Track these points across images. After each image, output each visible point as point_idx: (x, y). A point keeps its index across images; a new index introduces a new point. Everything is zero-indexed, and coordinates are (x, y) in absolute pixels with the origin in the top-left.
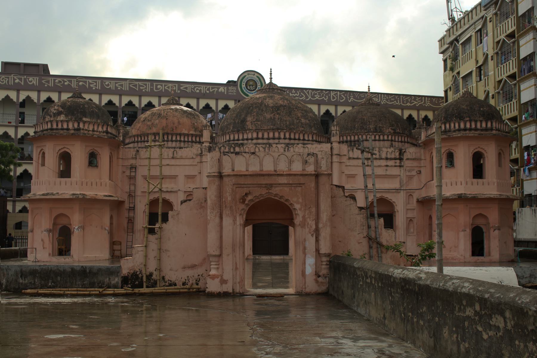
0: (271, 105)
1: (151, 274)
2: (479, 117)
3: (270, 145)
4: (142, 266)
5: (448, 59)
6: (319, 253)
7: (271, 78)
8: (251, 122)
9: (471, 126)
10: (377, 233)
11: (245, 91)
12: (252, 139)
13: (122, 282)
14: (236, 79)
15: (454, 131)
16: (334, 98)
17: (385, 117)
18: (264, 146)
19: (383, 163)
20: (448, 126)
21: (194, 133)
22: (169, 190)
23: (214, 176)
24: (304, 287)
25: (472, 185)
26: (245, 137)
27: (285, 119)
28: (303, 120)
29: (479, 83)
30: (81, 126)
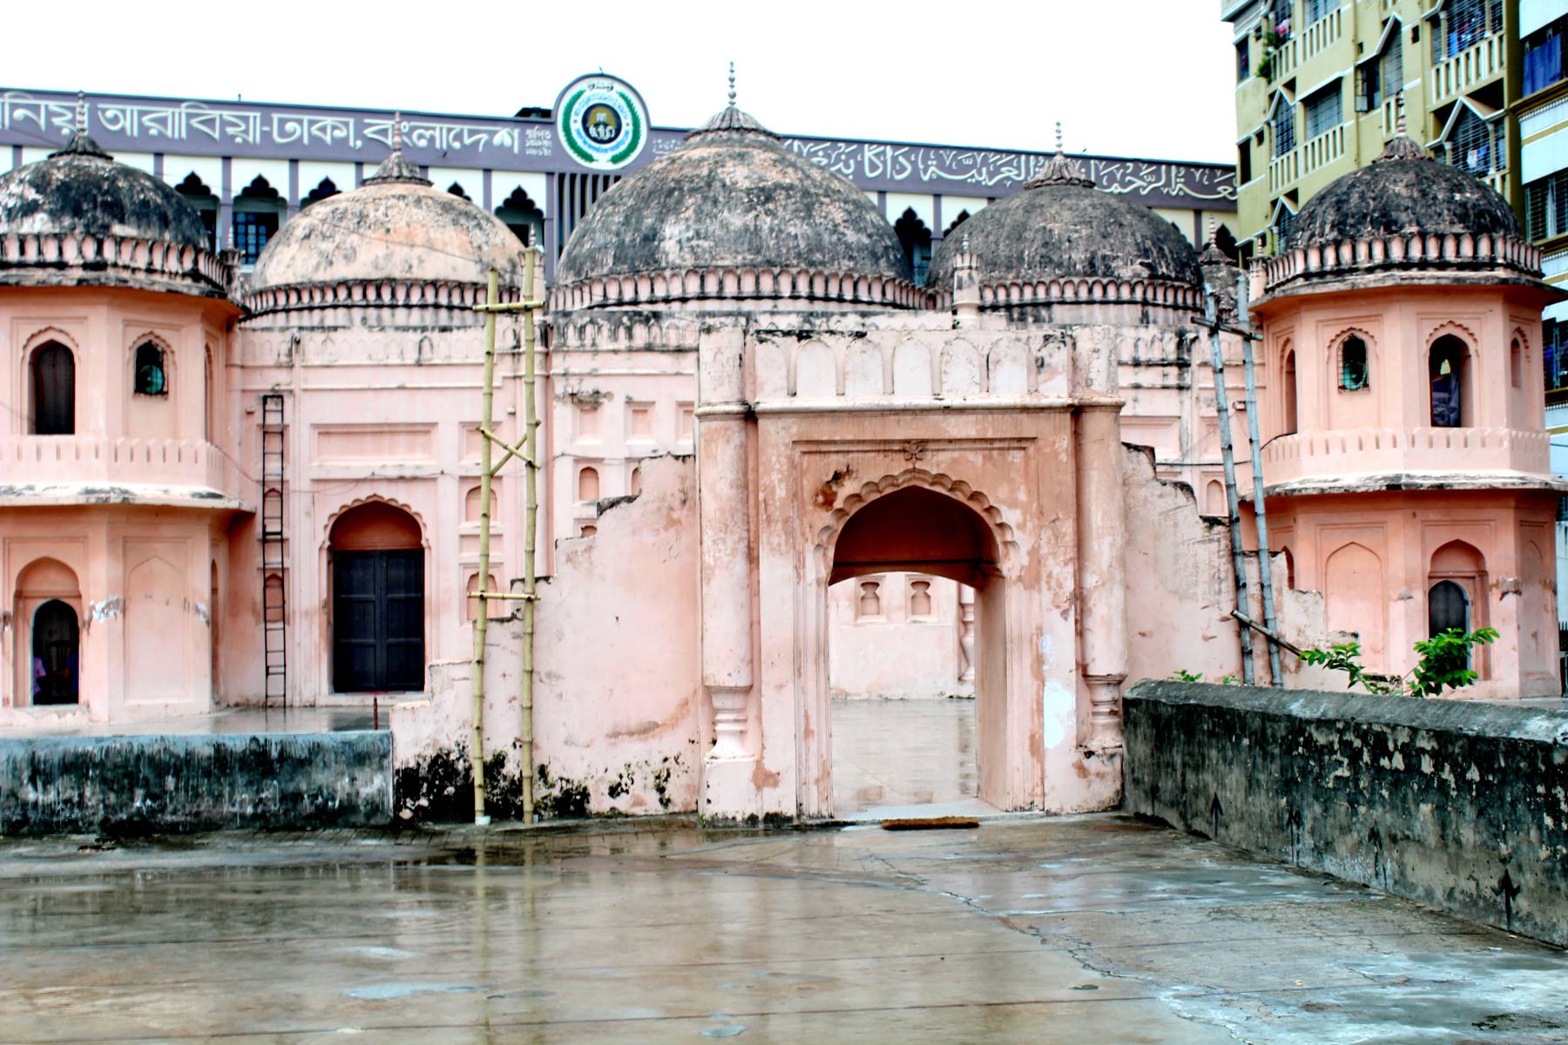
0: (746, 184)
1: (499, 761)
2: (1452, 223)
4: (470, 732)
5: (1252, 41)
6: (1086, 676)
8: (680, 241)
9: (1424, 251)
10: (1267, 603)
11: (580, 143)
12: (684, 300)
13: (397, 788)
14: (547, 105)
15: (1370, 270)
16: (873, 167)
17: (1121, 225)
20: (1346, 252)
22: (407, 473)
23: (727, 413)
24: (1038, 790)
25: (1431, 445)
26: (660, 292)
27: (793, 230)
28: (851, 236)
29: (1363, 118)
30: (109, 252)
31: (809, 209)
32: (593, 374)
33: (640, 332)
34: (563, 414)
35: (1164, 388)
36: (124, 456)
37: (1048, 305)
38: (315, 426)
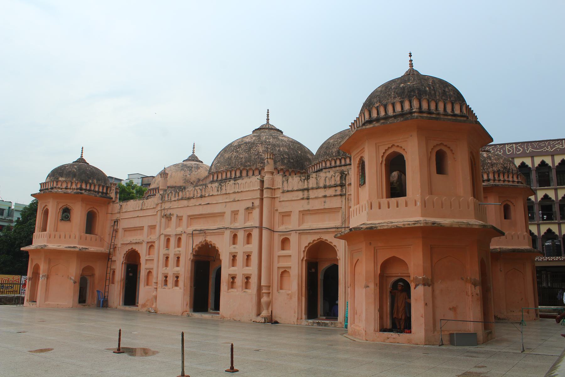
2: (395, 97)
3: (206, 185)
7: (268, 120)
16: (509, 151)
18: (201, 187)
19: (321, 193)
21: (184, 185)
22: (137, 241)
25: (380, 208)
27: (241, 156)
31: (250, 148)
32: (170, 208)
33: (181, 193)
34: (163, 220)
35: (335, 196)
36: (52, 237)
38: (123, 229)
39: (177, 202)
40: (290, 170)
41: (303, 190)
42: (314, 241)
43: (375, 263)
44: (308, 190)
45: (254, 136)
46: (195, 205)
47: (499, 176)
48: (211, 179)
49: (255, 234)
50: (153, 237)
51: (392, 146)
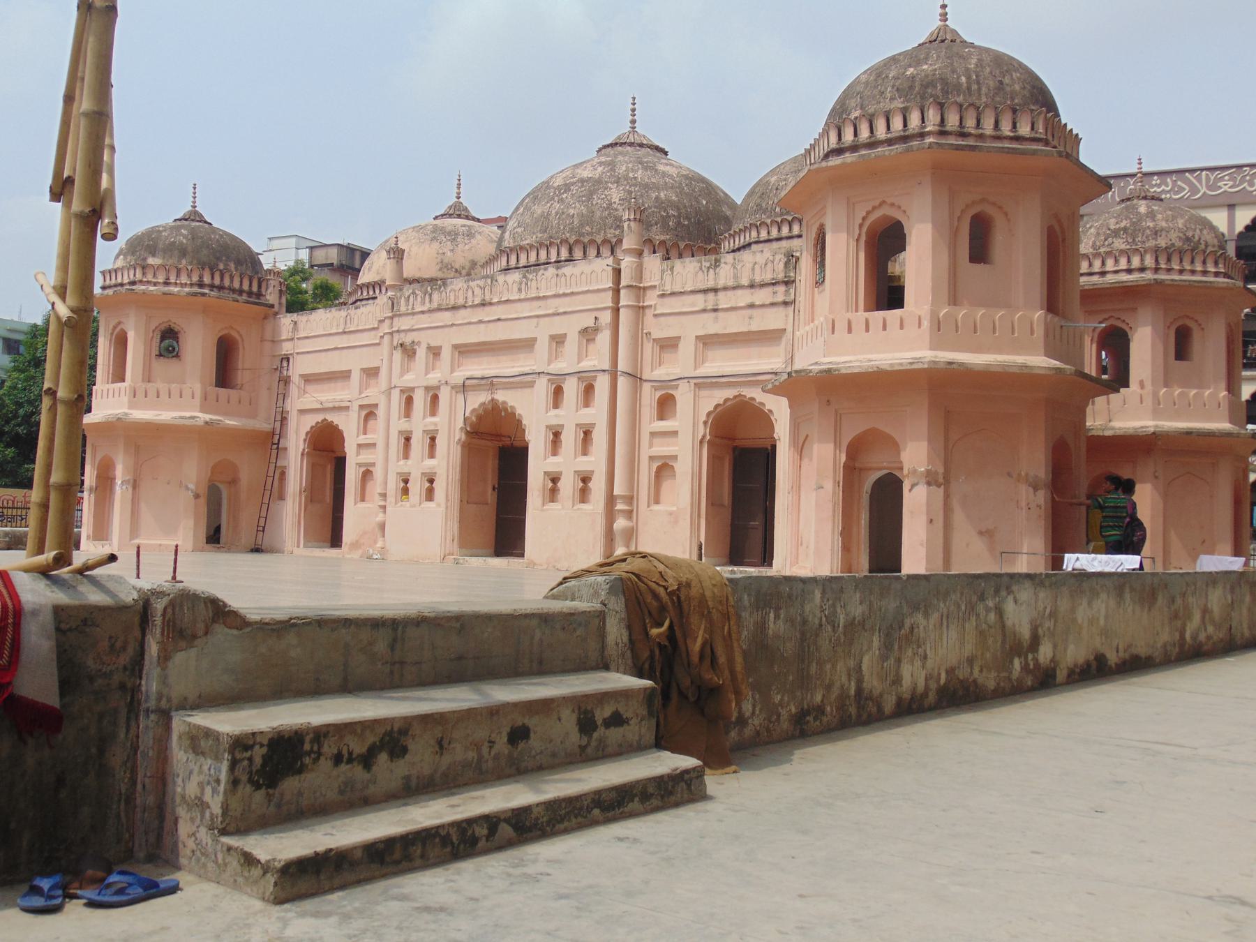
2: (892, 99)
18: (481, 283)
19: (743, 298)
21: (440, 275)
22: (337, 404)
25: (850, 331)
27: (572, 211)
34: (398, 355)
35: (773, 304)
36: (140, 394)
37: (749, 245)
39: (426, 315)
40: (682, 245)
41: (705, 291)
42: (726, 400)
43: (837, 444)
44: (715, 290)
45: (601, 164)
46: (470, 323)
47: (1169, 260)
48: (504, 263)
49: (602, 384)
50: (373, 394)
51: (880, 205)
